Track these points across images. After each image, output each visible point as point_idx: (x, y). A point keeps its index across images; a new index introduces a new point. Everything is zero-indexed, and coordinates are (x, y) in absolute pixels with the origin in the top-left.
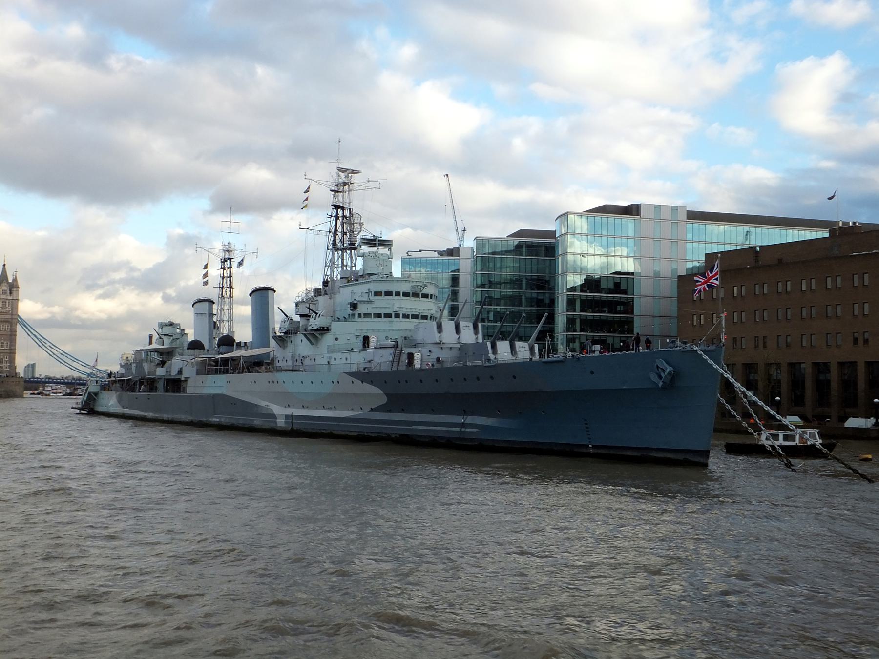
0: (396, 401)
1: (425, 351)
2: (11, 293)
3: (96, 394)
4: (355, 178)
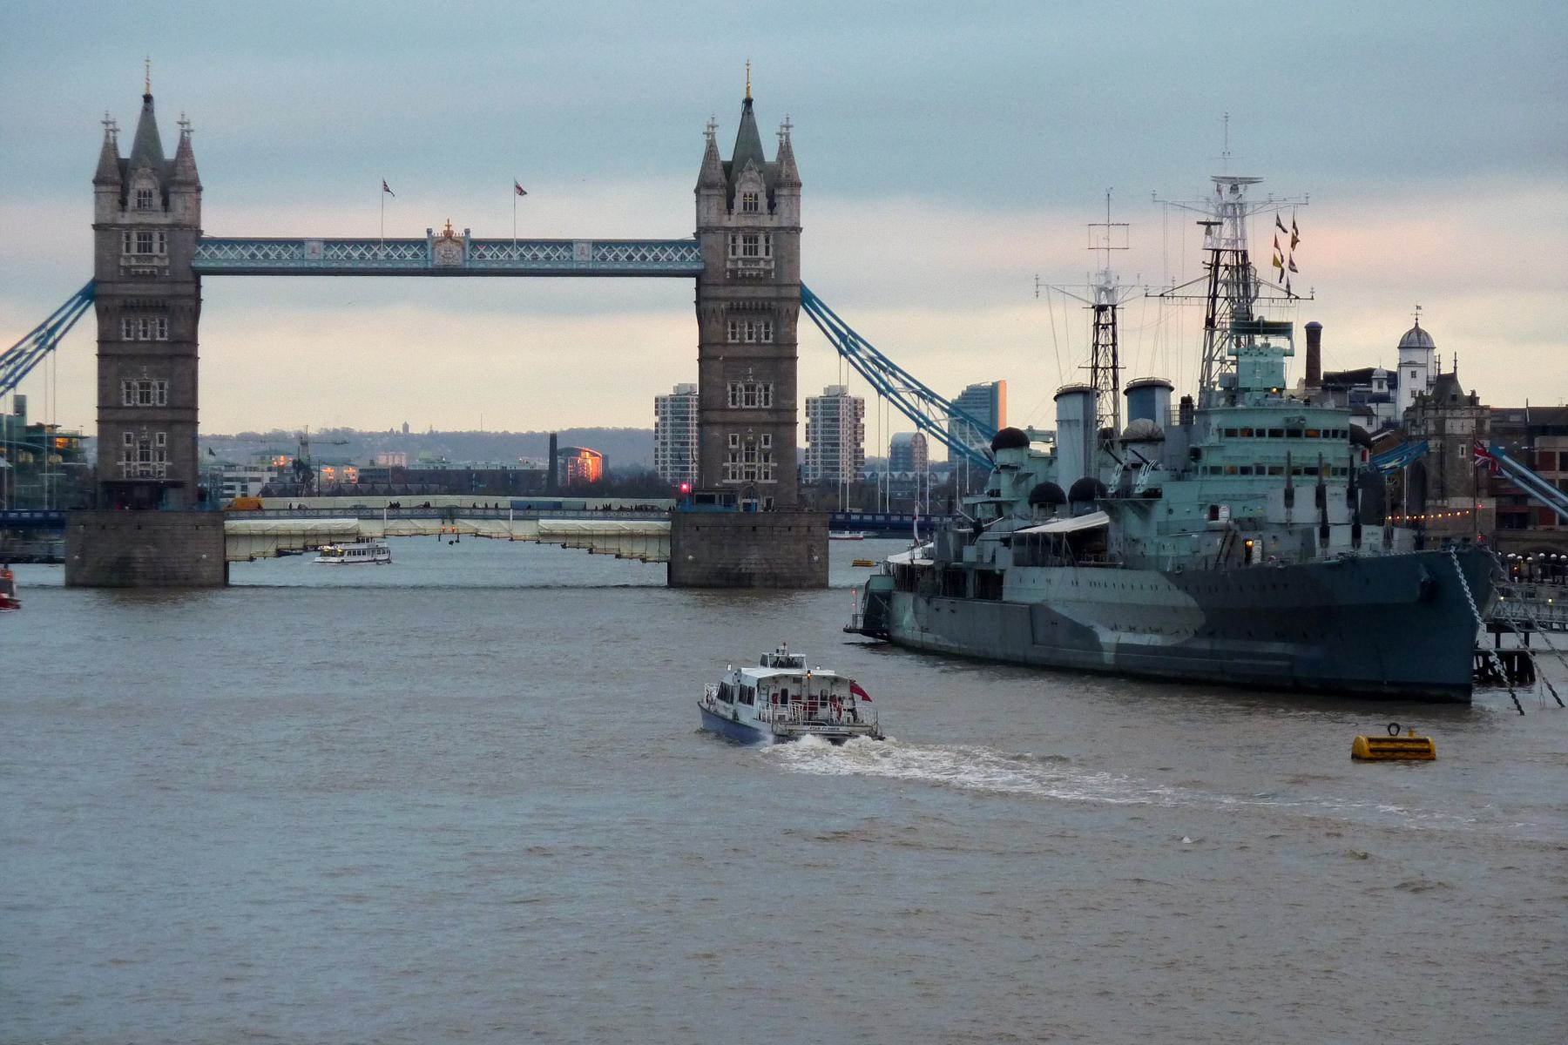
0: (1218, 623)
1: (1267, 535)
2: (772, 206)
3: (887, 597)
4: (1250, 194)
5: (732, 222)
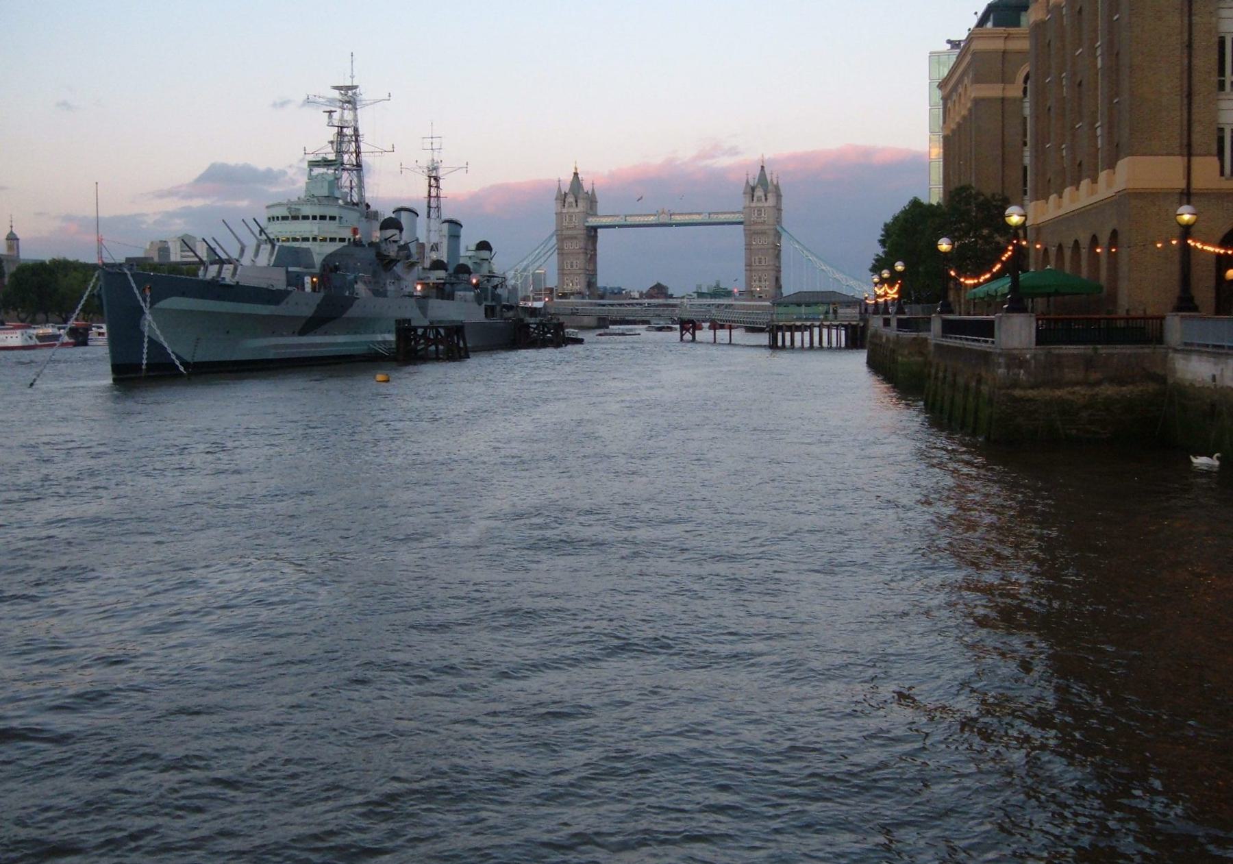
5: (753, 205)
